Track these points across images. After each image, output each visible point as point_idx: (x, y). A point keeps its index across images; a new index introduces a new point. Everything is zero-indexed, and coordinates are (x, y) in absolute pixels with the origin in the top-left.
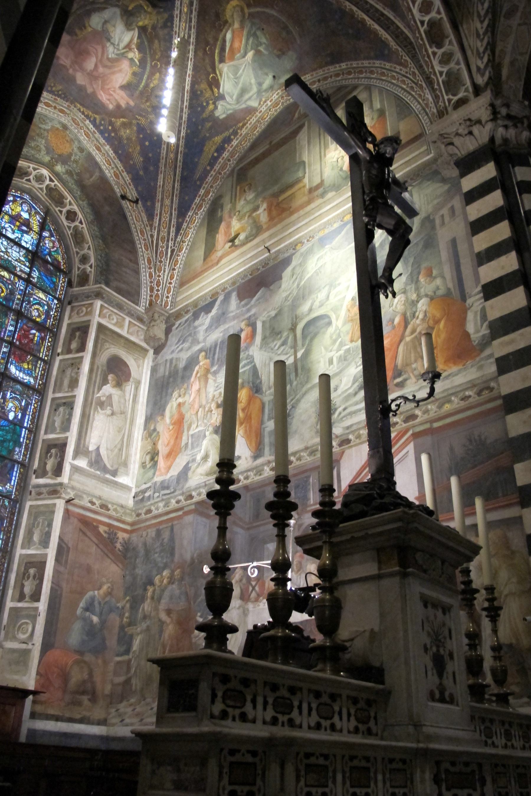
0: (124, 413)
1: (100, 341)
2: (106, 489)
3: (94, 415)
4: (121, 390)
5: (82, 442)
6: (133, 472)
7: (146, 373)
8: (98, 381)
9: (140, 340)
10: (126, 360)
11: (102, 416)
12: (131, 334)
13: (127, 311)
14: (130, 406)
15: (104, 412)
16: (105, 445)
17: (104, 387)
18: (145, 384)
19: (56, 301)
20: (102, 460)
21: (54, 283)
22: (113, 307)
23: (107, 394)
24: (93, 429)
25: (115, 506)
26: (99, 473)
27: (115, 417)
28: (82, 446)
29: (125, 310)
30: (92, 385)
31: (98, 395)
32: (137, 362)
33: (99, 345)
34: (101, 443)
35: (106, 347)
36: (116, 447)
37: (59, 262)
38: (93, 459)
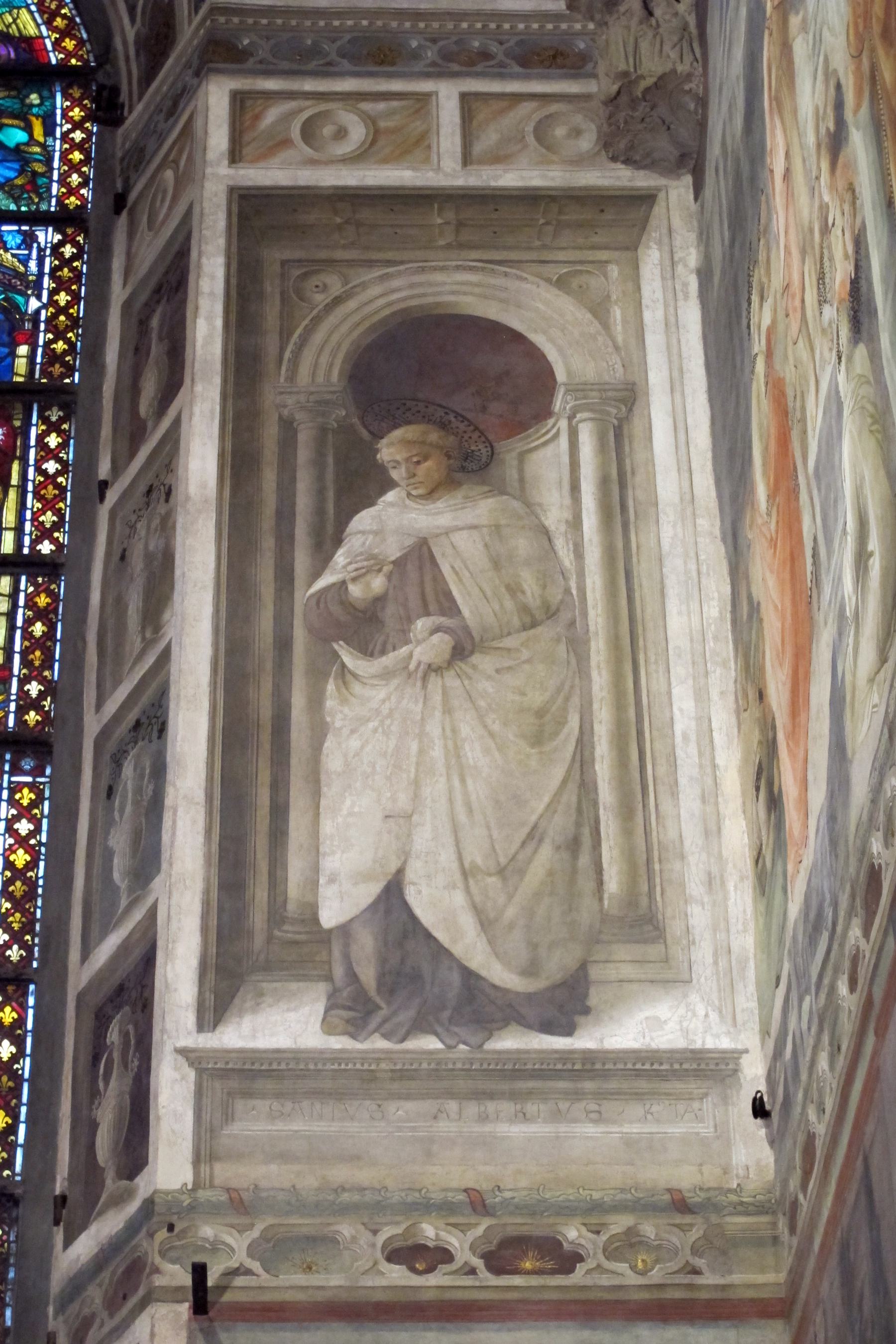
0: (551, 613)
1: (271, 287)
2: (517, 1131)
3: (316, 702)
4: (501, 490)
5: (260, 894)
6: (723, 951)
7: (672, 326)
8: (303, 502)
9: (579, 161)
10: (491, 311)
11: (378, 694)
12: (497, 158)
13: (430, 54)
14: (593, 555)
15: (389, 660)
16: (447, 857)
17: (363, 520)
18: (676, 385)
19: (47, 236)
20: (439, 952)
21: (18, 153)
22: (327, 71)
23: (393, 550)
24: (329, 793)
25: (619, 1223)
26: (431, 1043)
27: (483, 662)
28: (258, 919)
29: (415, 55)
30: (268, 543)
31: (326, 580)
32: (580, 295)
33: (271, 314)
34: (406, 855)
35: (320, 299)
36: (534, 836)
37: (29, 44)
38: (368, 975)
